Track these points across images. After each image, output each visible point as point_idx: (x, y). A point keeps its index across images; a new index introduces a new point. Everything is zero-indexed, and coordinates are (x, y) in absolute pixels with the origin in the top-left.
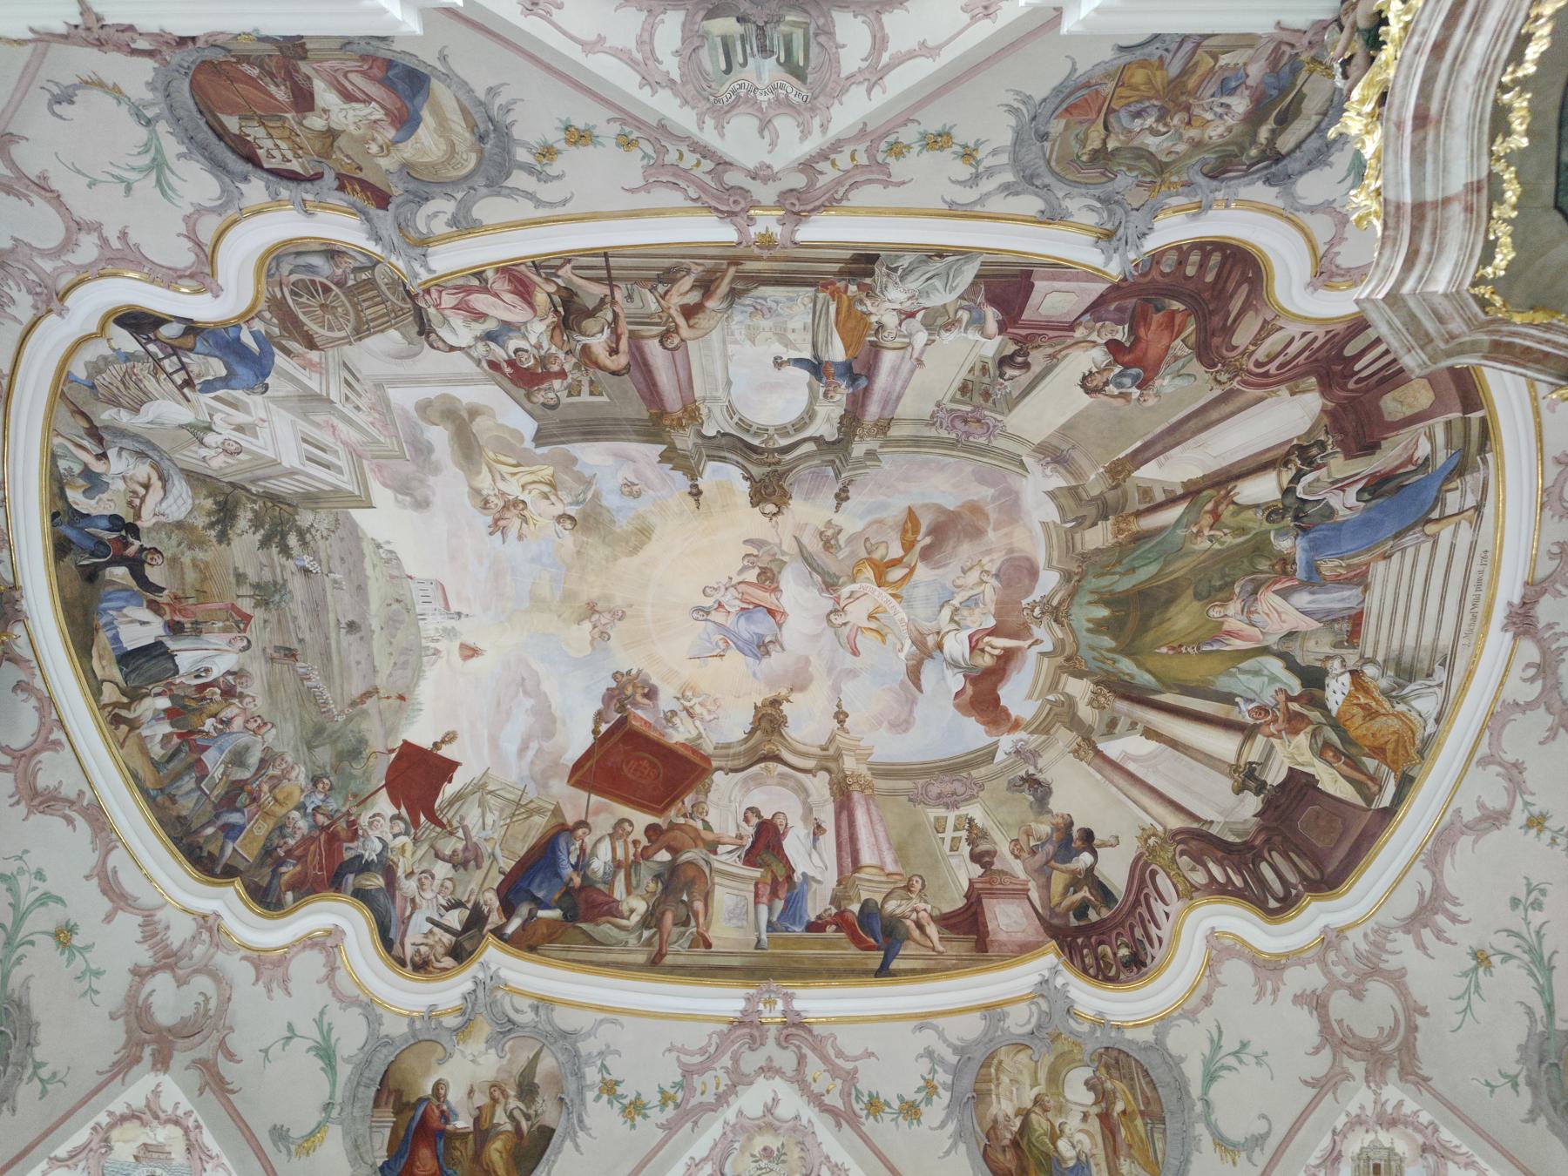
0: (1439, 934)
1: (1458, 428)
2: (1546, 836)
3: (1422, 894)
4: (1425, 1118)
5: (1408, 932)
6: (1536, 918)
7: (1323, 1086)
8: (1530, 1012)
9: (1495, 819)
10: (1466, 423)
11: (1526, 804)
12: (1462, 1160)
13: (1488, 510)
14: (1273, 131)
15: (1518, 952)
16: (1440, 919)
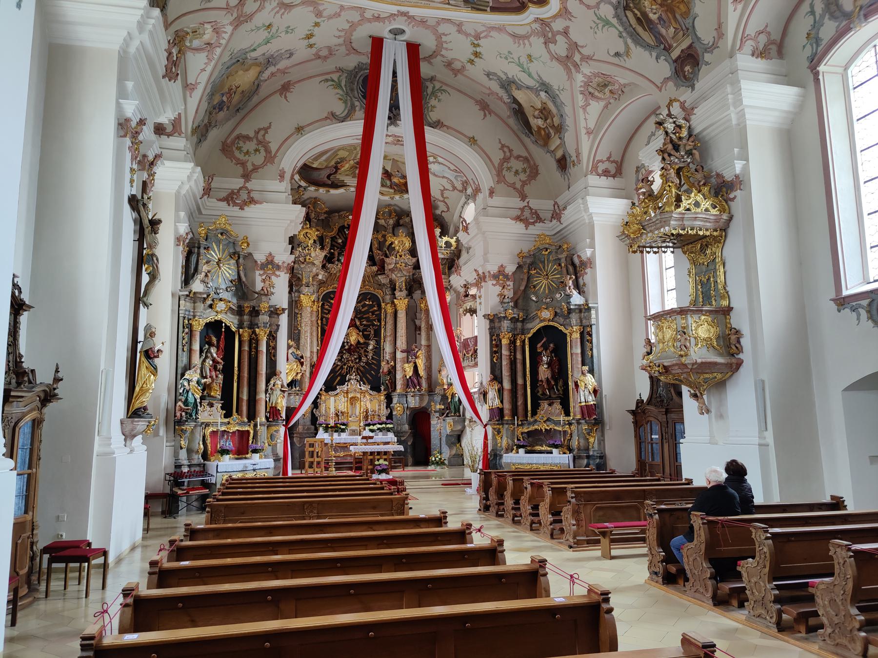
0: (278, 12)
1: (487, 4)
2: (312, 28)
3: (292, 3)
4: (223, 42)
5: (278, 4)
6: (283, 35)
7: (228, 8)
8: (252, 45)
9: (319, 14)
10: (488, 7)
11: (324, 21)
12: (210, 57)
13: (447, 6)
14: (636, 15)
15: (271, 34)
16: (283, 10)
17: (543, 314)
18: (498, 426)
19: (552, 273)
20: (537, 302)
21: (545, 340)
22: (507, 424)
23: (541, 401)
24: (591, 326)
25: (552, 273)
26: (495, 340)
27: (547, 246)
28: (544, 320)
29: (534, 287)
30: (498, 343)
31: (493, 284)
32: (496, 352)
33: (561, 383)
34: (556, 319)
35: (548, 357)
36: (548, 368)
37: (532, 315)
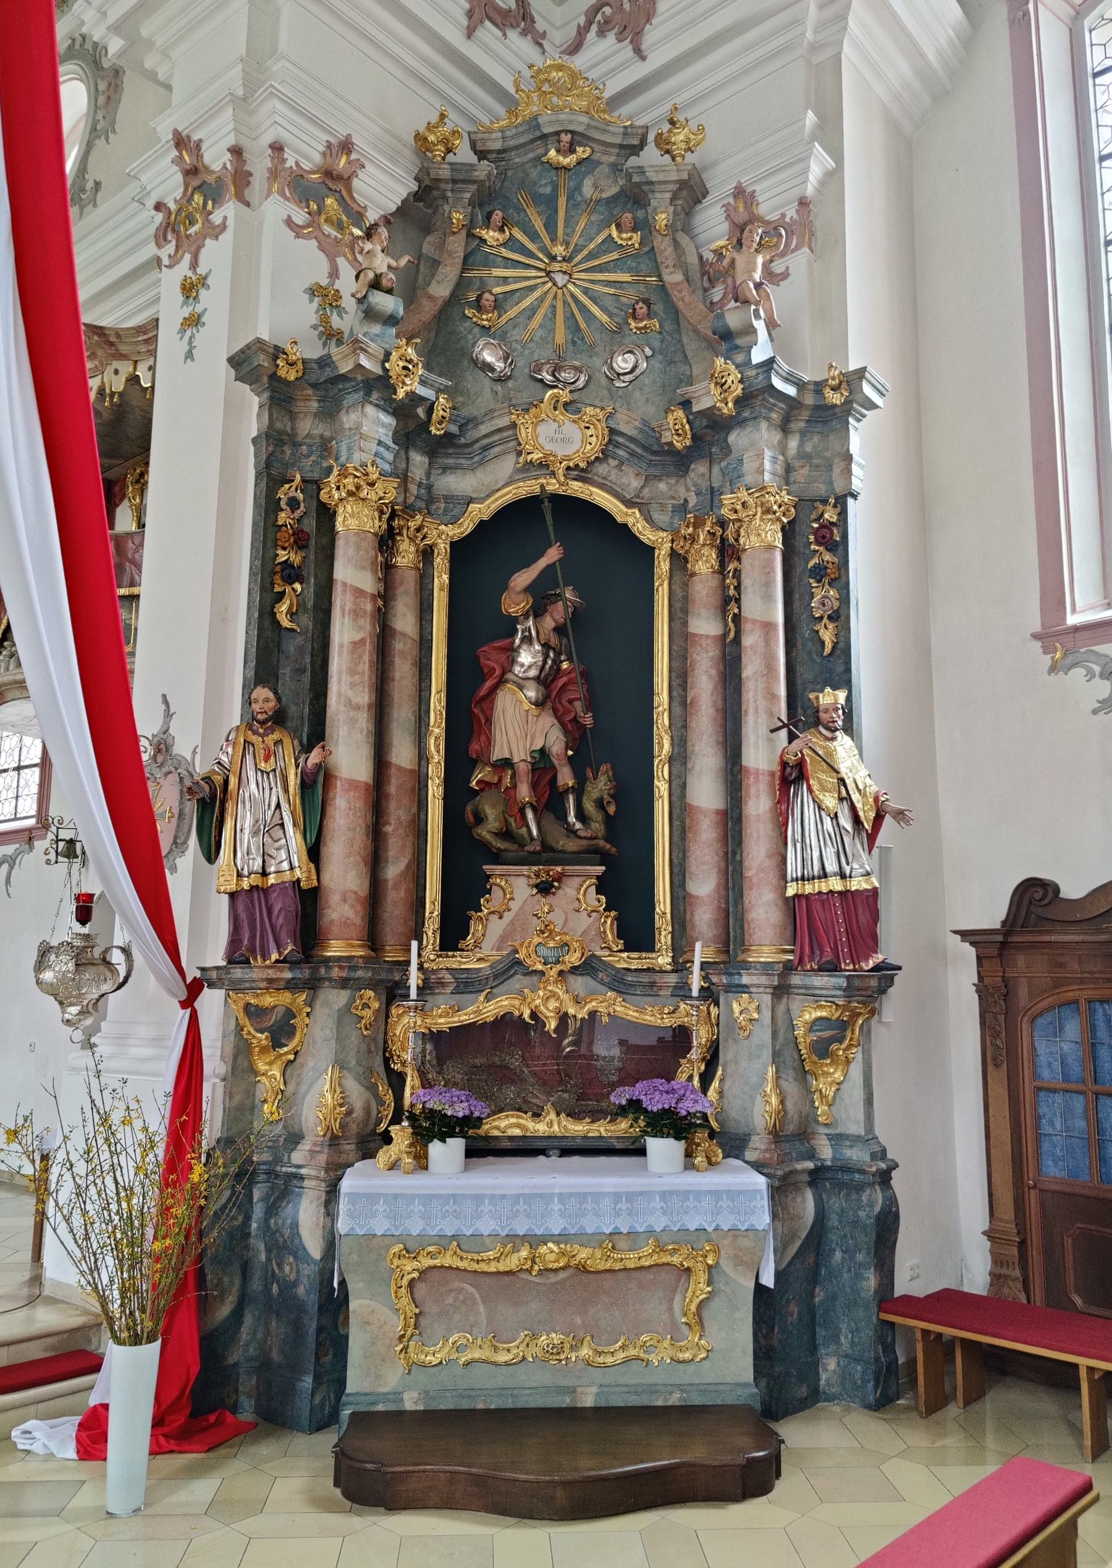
17: (546, 431)
18: (286, 998)
19: (591, 256)
20: (501, 380)
21: (553, 554)
22: (344, 983)
23: (499, 869)
24: (841, 503)
25: (591, 256)
26: (293, 503)
27: (580, 123)
28: (544, 466)
29: (499, 305)
30: (310, 525)
31: (289, 222)
32: (291, 574)
33: (600, 786)
34: (601, 469)
35: (546, 646)
36: (539, 704)
37: (484, 429)
